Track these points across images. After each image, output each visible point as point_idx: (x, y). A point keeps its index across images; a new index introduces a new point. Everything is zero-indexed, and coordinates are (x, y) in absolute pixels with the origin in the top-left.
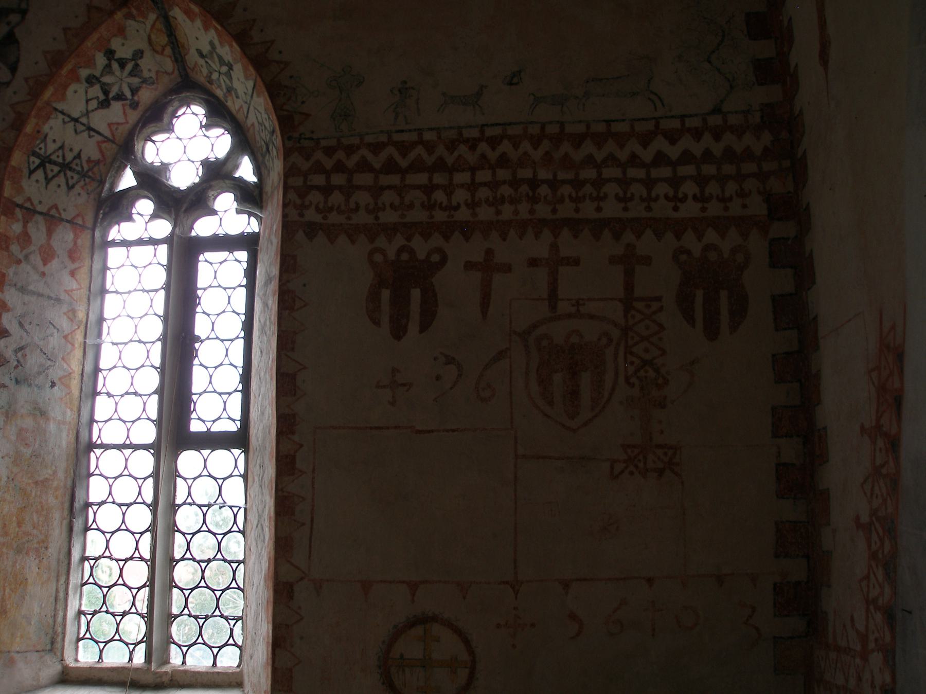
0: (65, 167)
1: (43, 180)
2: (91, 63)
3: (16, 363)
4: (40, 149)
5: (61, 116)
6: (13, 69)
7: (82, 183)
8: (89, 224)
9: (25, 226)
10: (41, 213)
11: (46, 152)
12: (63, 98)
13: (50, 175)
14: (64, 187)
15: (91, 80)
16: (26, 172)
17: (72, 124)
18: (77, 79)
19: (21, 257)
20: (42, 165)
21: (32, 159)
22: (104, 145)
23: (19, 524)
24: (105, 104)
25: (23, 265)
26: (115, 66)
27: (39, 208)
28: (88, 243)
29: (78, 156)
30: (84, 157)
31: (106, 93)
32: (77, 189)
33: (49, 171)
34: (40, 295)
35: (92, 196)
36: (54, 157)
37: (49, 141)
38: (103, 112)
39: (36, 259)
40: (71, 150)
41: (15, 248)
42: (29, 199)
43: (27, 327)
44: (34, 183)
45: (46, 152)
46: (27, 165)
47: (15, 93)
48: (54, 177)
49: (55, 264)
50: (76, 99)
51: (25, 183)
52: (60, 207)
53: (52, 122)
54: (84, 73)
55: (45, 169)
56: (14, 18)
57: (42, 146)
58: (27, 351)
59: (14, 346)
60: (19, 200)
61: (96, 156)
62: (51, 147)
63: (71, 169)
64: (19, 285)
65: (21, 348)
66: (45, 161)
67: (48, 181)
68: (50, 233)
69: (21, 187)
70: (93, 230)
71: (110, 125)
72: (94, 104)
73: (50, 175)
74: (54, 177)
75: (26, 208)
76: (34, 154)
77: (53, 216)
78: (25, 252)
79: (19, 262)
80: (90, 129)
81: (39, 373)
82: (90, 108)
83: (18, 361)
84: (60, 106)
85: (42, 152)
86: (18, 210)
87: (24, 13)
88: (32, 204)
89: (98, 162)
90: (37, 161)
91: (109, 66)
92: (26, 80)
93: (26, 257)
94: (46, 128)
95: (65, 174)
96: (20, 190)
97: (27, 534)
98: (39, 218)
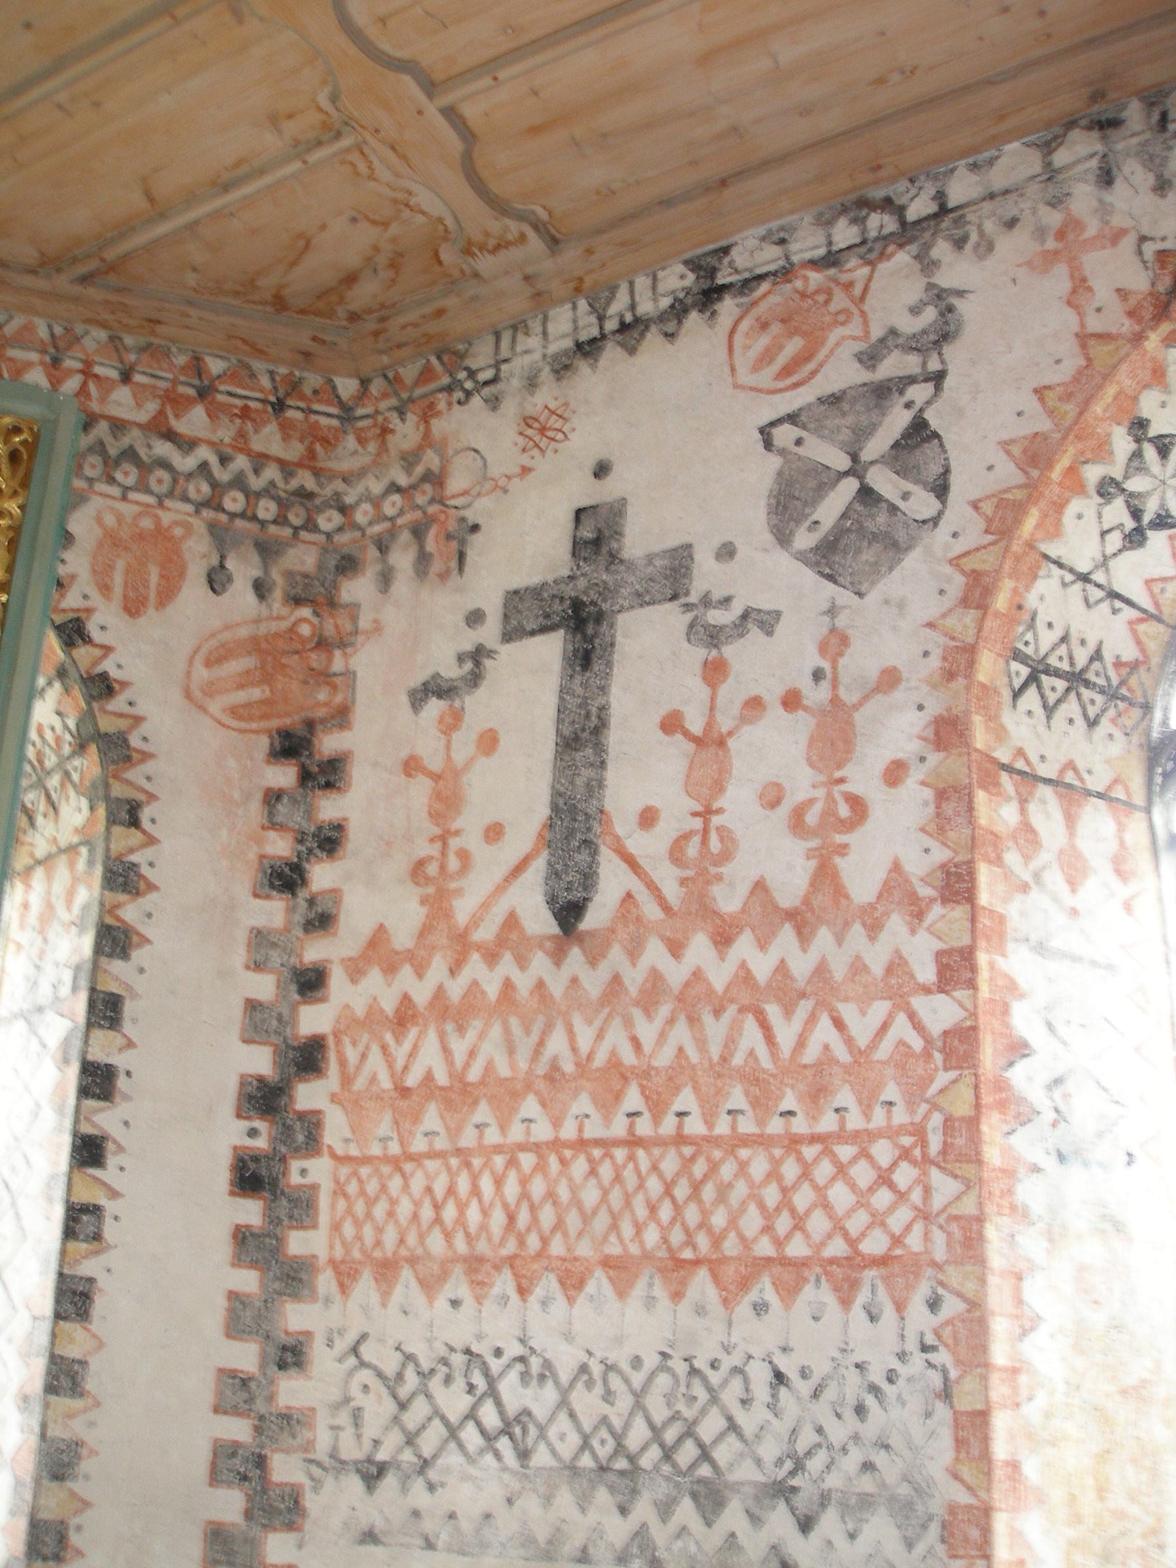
0: (1076, 679)
1: (1039, 712)
2: (1102, 451)
3: (1053, 1115)
4: (1026, 643)
5: (1056, 571)
6: (941, 489)
7: (1111, 713)
8: (1139, 799)
9: (1023, 811)
10: (1048, 781)
11: (1037, 650)
12: (1056, 532)
13: (1052, 698)
14: (1080, 722)
15: (1108, 489)
16: (1007, 695)
17: (1079, 586)
18: (1080, 488)
19: (1026, 876)
20: (1033, 678)
21: (1015, 666)
22: (1142, 628)
23: (1101, 1492)
24: (1135, 538)
25: (1034, 894)
26: (1150, 452)
27: (1043, 771)
28: (1144, 840)
29: (1097, 656)
30: (1108, 656)
31: (1136, 514)
32: (1105, 727)
33: (1048, 692)
34: (1076, 959)
35: (1135, 739)
36: (1053, 661)
37: (1040, 624)
38: (1132, 557)
39: (1055, 879)
40: (1083, 642)
41: (1012, 858)
42: (1020, 752)
43: (1061, 1029)
44: (1026, 719)
45: (1037, 650)
46: (1006, 680)
47: (955, 535)
48: (1059, 701)
49: (1091, 888)
50: (1083, 531)
51: (1008, 718)
52: (1081, 765)
53: (1041, 586)
54: (1093, 474)
55: (1039, 687)
56: (919, 393)
57: (1029, 637)
58: (1070, 1085)
59: (1046, 1077)
60: (1003, 755)
61: (1129, 653)
62: (1047, 639)
63: (1087, 684)
64: (1034, 938)
65: (1058, 1081)
66: (1038, 671)
67: (1050, 710)
68: (1071, 821)
69: (1003, 728)
70: (1148, 810)
71: (1149, 583)
72: (1115, 541)
73: (1052, 698)
74: (1059, 701)
75: (1020, 772)
76: (1018, 656)
77: (1070, 786)
78: (1033, 865)
79: (1025, 888)
80: (1114, 595)
81: (1100, 1135)
82: (1110, 550)
83: (1057, 1110)
84: (1053, 550)
85: (1029, 651)
86: (1004, 777)
87: (938, 378)
88: (1028, 762)
89: (1134, 666)
90: (1025, 671)
91: (1137, 455)
92: (975, 506)
93: (1037, 876)
94: (1031, 600)
95: (1078, 695)
96: (1001, 733)
97: (1120, 1515)
98: (1045, 791)
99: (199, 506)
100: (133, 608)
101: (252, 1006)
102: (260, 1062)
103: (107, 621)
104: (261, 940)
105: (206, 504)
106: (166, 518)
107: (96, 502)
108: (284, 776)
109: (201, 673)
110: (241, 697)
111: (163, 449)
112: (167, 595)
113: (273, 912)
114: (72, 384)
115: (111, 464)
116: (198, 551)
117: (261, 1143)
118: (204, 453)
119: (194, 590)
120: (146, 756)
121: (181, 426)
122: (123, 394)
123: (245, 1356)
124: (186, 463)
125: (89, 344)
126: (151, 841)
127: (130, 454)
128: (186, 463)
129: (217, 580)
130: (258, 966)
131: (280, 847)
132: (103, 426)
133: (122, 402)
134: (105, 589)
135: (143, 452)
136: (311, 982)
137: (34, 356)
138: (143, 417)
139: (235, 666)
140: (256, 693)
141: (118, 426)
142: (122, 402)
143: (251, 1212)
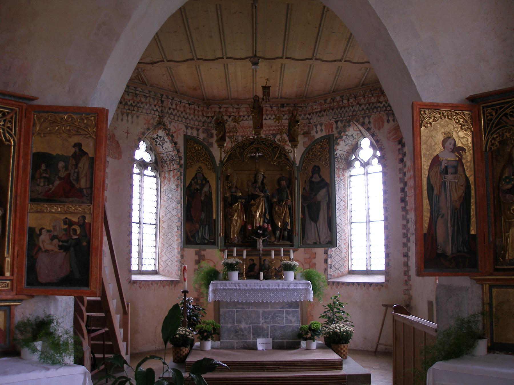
99: (384, 111)
100: (379, 129)
101: (400, 178)
102: (402, 185)
103: (377, 132)
104: (400, 170)
105: (385, 110)
106: (381, 115)
107: (372, 116)
108: (399, 147)
109: (389, 135)
110: (394, 137)
111: (379, 104)
112: (383, 125)
113: (401, 166)
114: (367, 99)
115: (373, 109)
116: (385, 118)
117: (403, 196)
118: (384, 103)
119: (386, 124)
120: (384, 149)
121: (380, 100)
122: (373, 98)
123: (404, 222)
124: (382, 105)
125: (367, 92)
126: (386, 160)
127: (375, 107)
128: (382, 105)
129: (388, 121)
130: (400, 173)
131: (401, 156)
132: (371, 104)
133: (373, 100)
134: (375, 128)
135: (376, 106)
136: (405, 174)
137: (361, 97)
138: (376, 101)
139: (392, 133)
140: (395, 136)
141: (373, 103)
142: (373, 100)
143: (403, 205)
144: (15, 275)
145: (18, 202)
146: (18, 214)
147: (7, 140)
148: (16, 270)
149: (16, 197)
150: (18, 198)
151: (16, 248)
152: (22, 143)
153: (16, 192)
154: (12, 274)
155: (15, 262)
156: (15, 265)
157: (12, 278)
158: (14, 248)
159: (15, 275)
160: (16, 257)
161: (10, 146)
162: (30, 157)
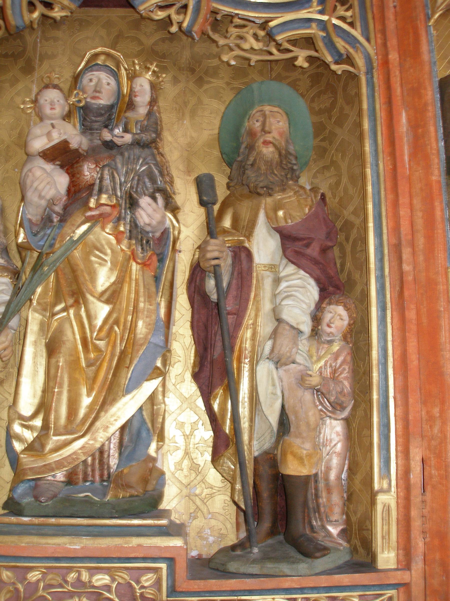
144: (418, 565)
145: (406, 267)
146: (411, 314)
147: (341, 59)
148: (419, 544)
149: (397, 249)
150: (406, 253)
151: (416, 455)
152: (394, 56)
153: (396, 229)
154: (406, 562)
155: (414, 513)
156: (416, 524)
157: (405, 577)
158: (405, 452)
159: (418, 565)
160: (416, 492)
161: (353, 78)
162: (432, 95)
